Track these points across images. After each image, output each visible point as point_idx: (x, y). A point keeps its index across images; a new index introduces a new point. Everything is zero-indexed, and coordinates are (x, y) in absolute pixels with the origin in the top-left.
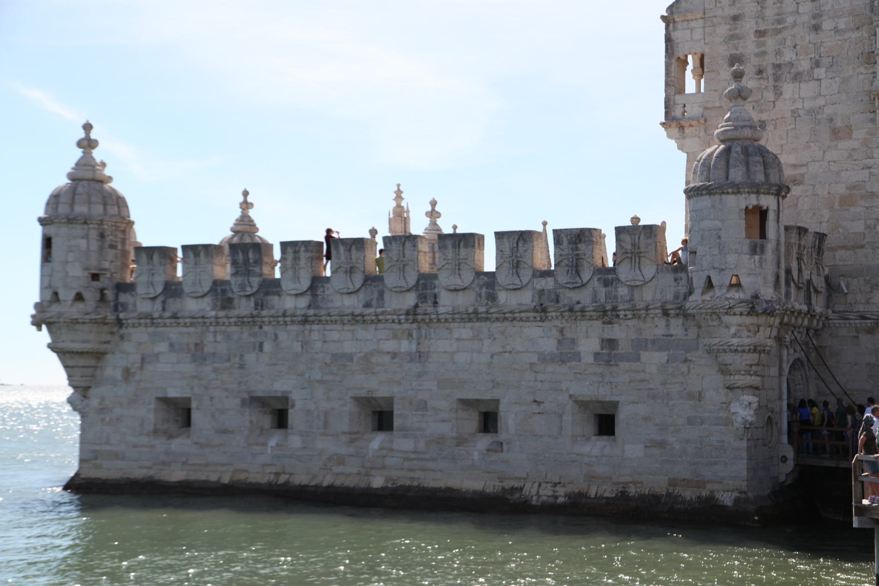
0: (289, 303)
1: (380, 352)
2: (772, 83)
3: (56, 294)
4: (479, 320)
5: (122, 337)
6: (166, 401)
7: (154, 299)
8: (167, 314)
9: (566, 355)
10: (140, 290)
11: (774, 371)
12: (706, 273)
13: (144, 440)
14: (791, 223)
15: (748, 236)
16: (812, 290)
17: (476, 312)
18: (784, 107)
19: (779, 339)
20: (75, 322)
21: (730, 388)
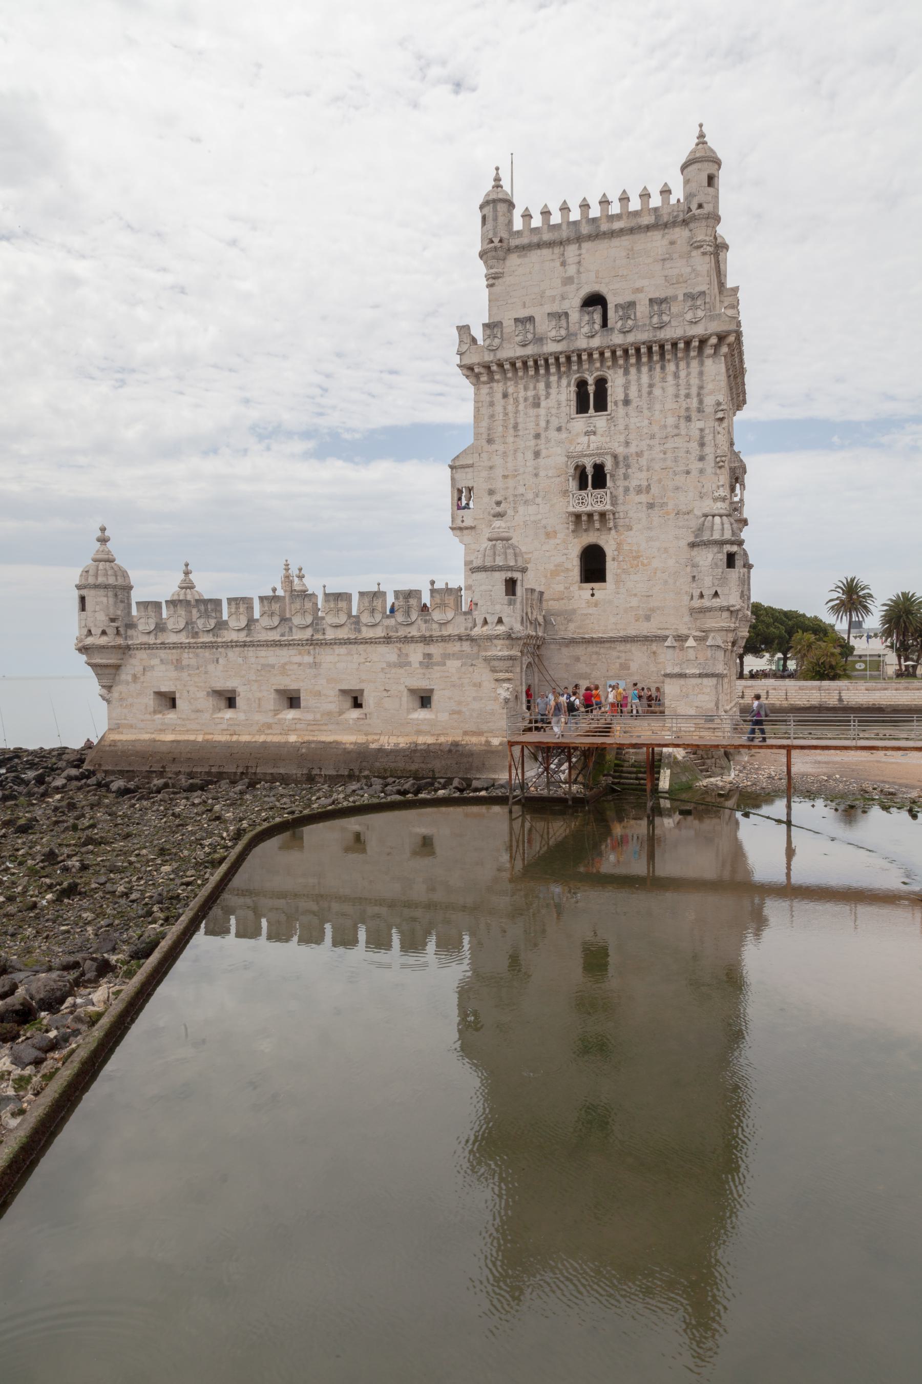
1: (291, 663)
2: (512, 505)
3: (90, 631)
4: (350, 643)
5: (130, 656)
6: (159, 694)
7: (149, 633)
8: (159, 641)
9: (403, 664)
10: (141, 627)
11: (518, 670)
12: (484, 616)
13: (148, 717)
14: (529, 587)
17: (348, 639)
20: (103, 647)
21: (496, 680)
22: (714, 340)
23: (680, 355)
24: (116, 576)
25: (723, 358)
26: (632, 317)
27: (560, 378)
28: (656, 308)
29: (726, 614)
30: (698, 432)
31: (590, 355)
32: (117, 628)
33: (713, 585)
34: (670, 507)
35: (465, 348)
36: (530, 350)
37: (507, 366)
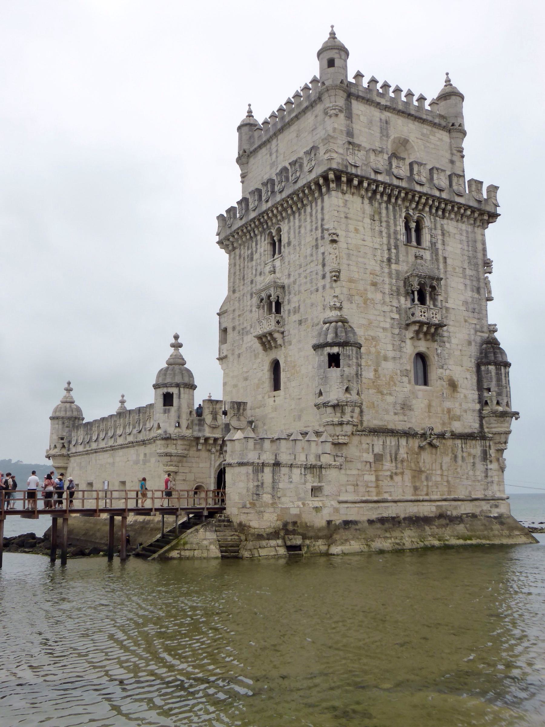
0: (94, 446)
7: (74, 446)
15: (164, 406)
16: (231, 427)
18: (244, 346)
19: (209, 451)
22: (321, 181)
23: (310, 198)
24: (66, 411)
25: (333, 193)
26: (284, 180)
27: (261, 236)
28: (293, 169)
29: (329, 410)
30: (321, 255)
31: (268, 214)
32: (63, 443)
33: (319, 385)
34: (309, 321)
35: (220, 229)
36: (243, 222)
37: (236, 236)
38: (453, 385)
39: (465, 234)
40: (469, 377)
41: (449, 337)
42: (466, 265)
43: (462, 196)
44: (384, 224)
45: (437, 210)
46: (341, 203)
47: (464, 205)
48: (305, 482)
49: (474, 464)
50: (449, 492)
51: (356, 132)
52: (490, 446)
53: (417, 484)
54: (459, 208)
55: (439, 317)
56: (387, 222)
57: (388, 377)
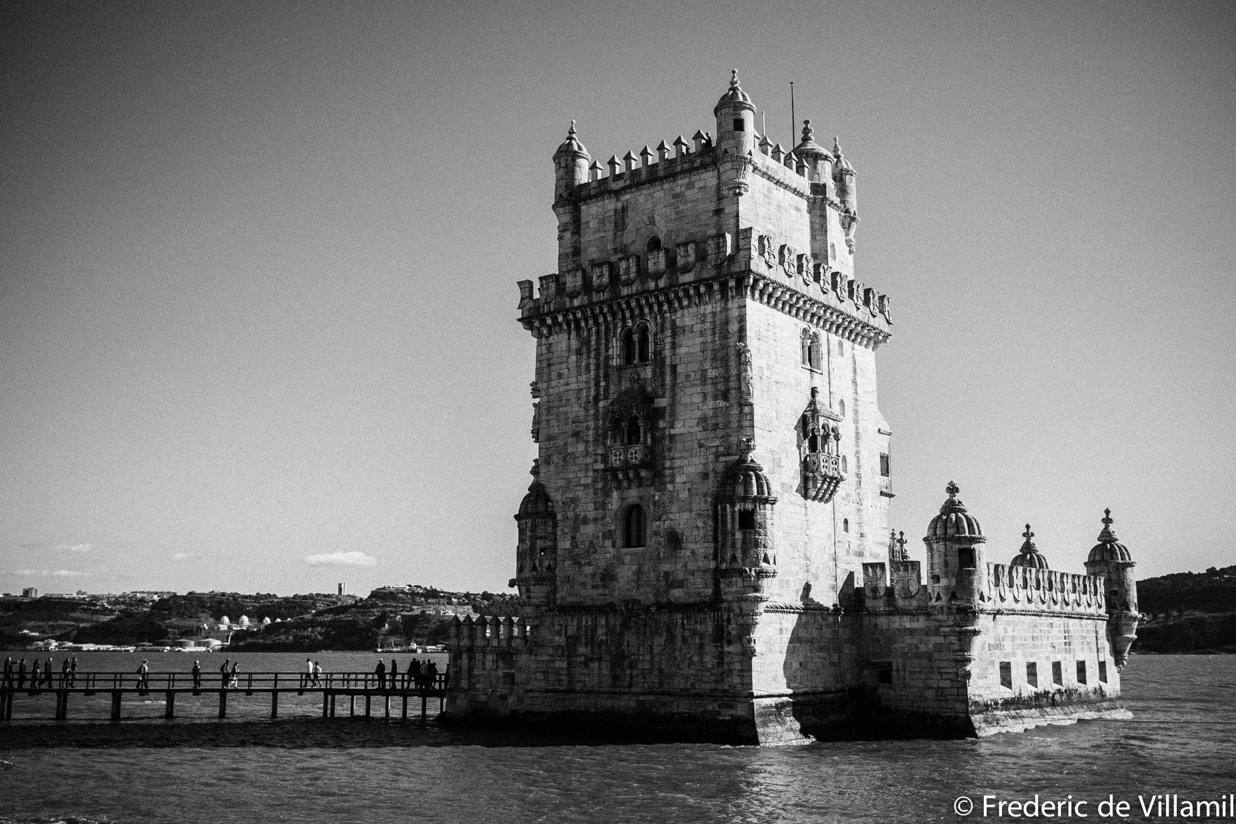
38: (675, 540)
39: (709, 319)
40: (700, 524)
41: (673, 476)
42: (707, 366)
43: (689, 271)
44: (592, 355)
45: (660, 305)
46: (544, 351)
47: (689, 283)
48: (498, 668)
49: (701, 646)
50: (661, 684)
51: (583, 246)
52: (729, 620)
53: (619, 672)
54: (686, 291)
55: (639, 456)
56: (597, 349)
57: (587, 544)
